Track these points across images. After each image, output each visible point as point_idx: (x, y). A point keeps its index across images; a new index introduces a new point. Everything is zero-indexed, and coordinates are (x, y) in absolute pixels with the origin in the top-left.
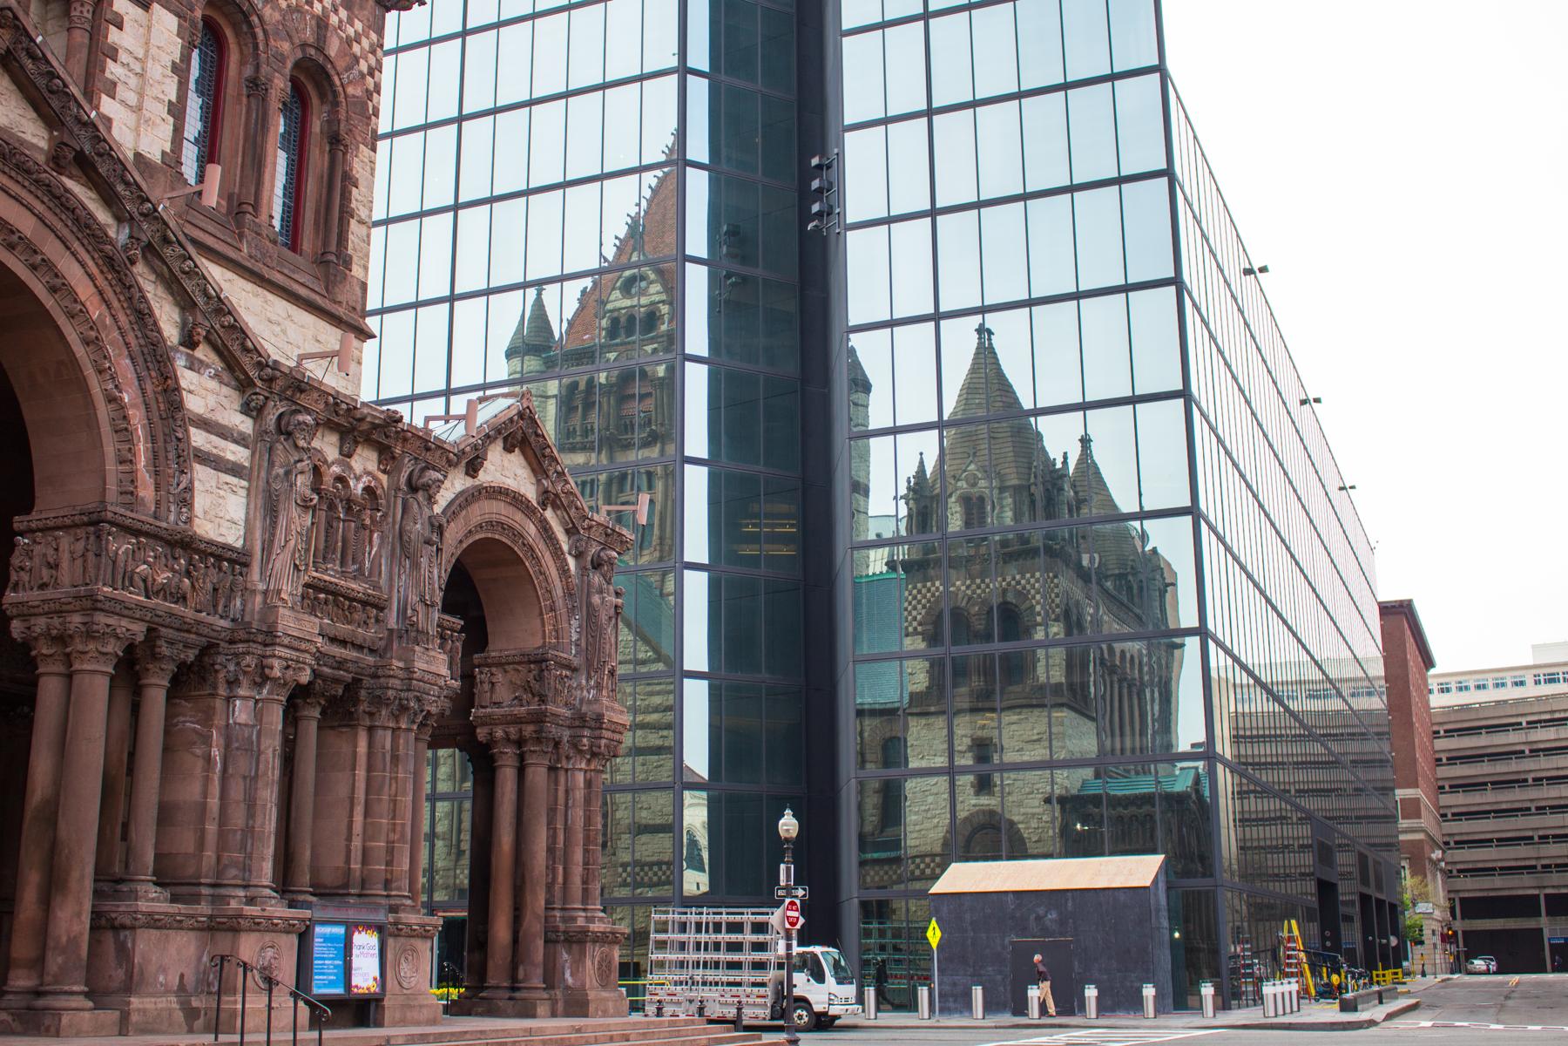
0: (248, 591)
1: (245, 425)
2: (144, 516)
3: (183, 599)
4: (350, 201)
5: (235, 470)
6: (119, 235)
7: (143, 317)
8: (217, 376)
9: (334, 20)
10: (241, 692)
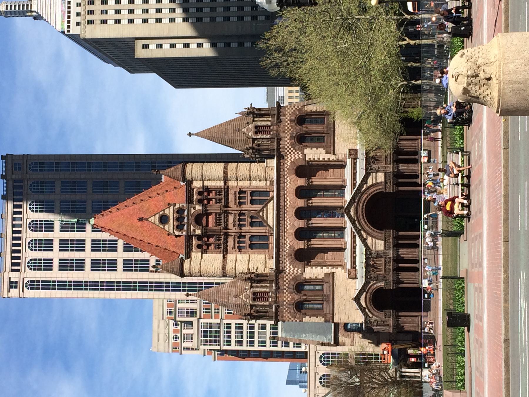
2: (384, 187)
3: (390, 181)
7: (365, 190)
9: (288, 118)
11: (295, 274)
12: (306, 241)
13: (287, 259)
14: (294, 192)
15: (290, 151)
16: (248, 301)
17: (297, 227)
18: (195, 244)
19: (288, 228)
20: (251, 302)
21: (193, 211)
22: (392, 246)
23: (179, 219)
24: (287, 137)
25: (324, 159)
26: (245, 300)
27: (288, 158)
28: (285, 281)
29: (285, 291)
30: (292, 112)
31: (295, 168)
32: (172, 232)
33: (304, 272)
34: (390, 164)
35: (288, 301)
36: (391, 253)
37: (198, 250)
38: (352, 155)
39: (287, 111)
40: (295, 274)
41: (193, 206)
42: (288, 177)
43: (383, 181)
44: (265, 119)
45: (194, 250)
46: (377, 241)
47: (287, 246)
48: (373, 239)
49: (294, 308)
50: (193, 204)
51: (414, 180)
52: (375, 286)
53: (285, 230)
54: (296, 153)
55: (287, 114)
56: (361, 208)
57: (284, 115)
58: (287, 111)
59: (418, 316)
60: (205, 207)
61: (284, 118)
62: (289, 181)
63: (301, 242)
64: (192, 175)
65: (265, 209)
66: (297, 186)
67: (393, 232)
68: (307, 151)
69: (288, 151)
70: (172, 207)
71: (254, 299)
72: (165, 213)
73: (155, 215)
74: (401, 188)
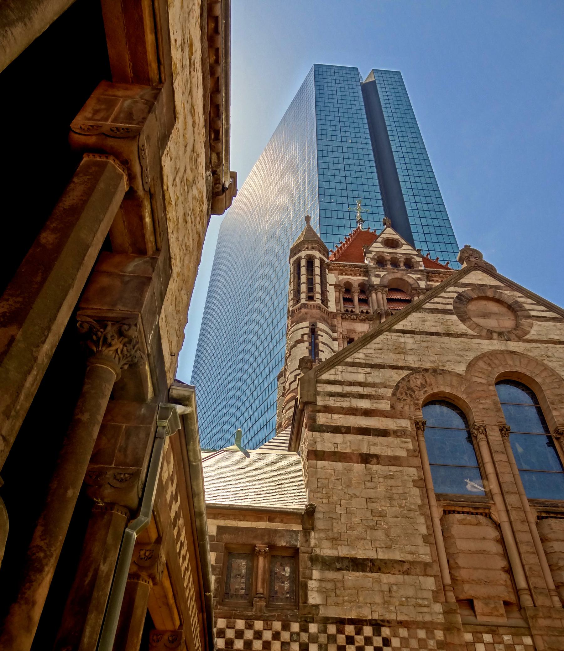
21: (414, 276)
32: (371, 249)
45: (341, 277)
72: (404, 244)
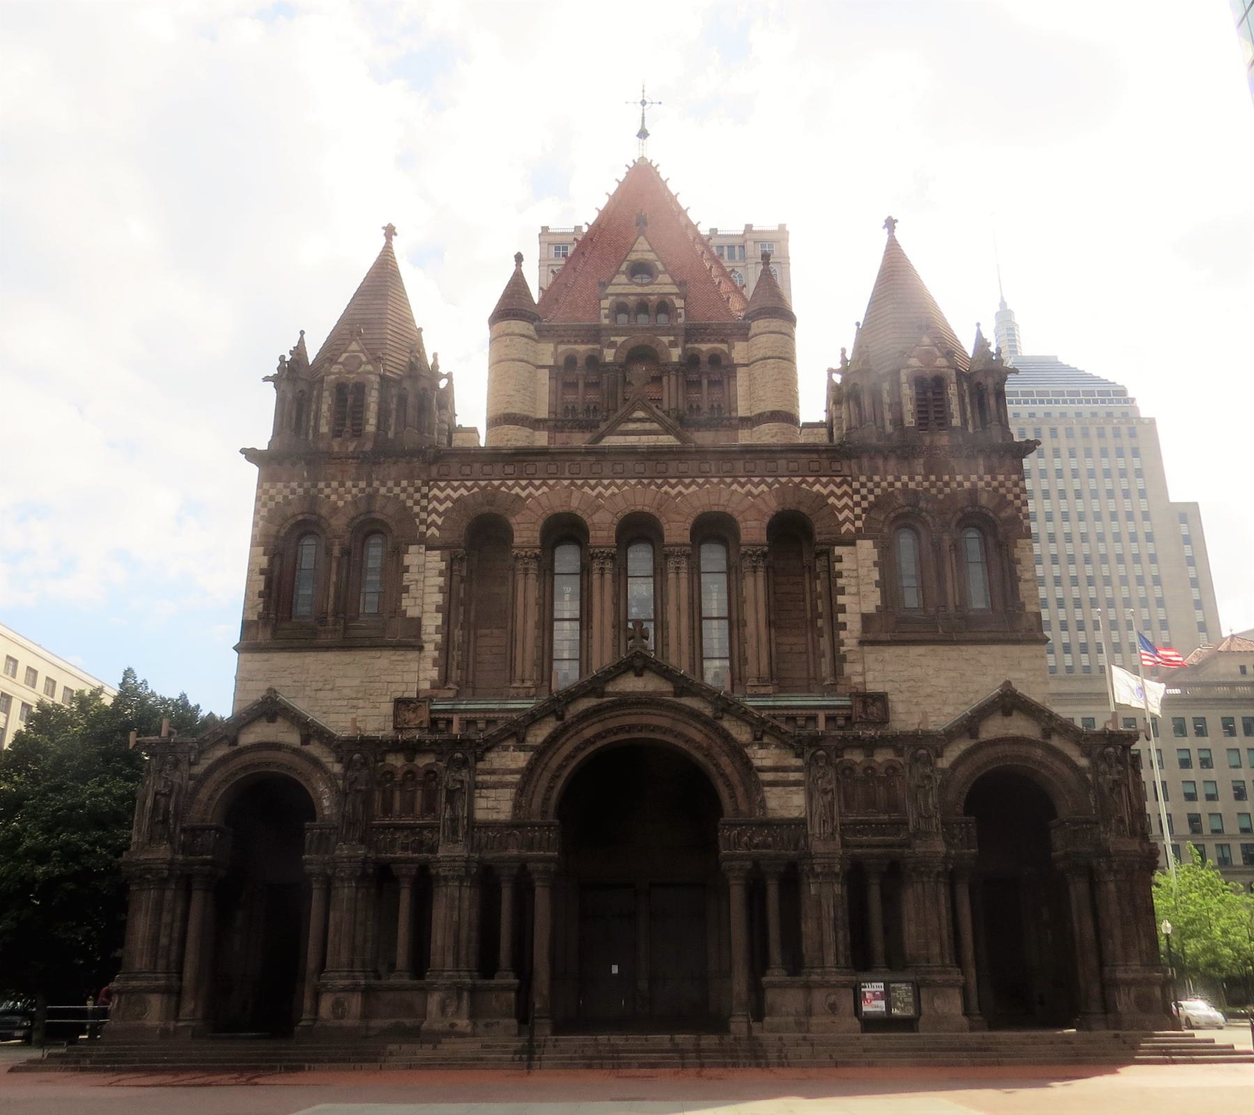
0: (806, 836)
1: (798, 762)
3: (769, 847)
4: (1016, 573)
5: (796, 783)
6: (708, 711)
7: (726, 737)
8: (777, 746)
9: (981, 484)
10: (811, 880)
11: (423, 515)
12: (537, 551)
13: (476, 489)
14: (715, 509)
15: (864, 491)
16: (335, 368)
17: (589, 522)
18: (578, 352)
19: (586, 489)
20: (333, 377)
22: (489, 855)
23: (643, 307)
24: (911, 479)
25: (844, 611)
26: (341, 360)
27: (839, 486)
28: (397, 484)
29: (362, 484)
30: (1004, 496)
31: (803, 509)
33: (427, 549)
34: (845, 845)
35: (328, 497)
36: (451, 852)
37: (561, 361)
38: (865, 711)
39: (1007, 479)
40: (423, 515)
41: (681, 340)
42: (770, 486)
43: (770, 815)
44: (969, 414)
45: (562, 348)
46: (508, 794)
47: (524, 489)
48: (518, 776)
49: (300, 518)
50: (686, 342)
51: (775, 954)
52: (322, 788)
53: (579, 482)
54: (858, 511)
55: (994, 479)
56: (655, 721)
57: (991, 471)
58: (1007, 479)
59: (181, 979)
60: (677, 371)
61: (981, 470)
62: (756, 492)
63: (537, 535)
64: (765, 333)
65: (655, 426)
66: (739, 519)
67: (550, 860)
68: (866, 548)
69: (863, 485)
70: (675, 290)
71: (341, 390)
72: (660, 272)
73: (652, 250)
74: (737, 894)
